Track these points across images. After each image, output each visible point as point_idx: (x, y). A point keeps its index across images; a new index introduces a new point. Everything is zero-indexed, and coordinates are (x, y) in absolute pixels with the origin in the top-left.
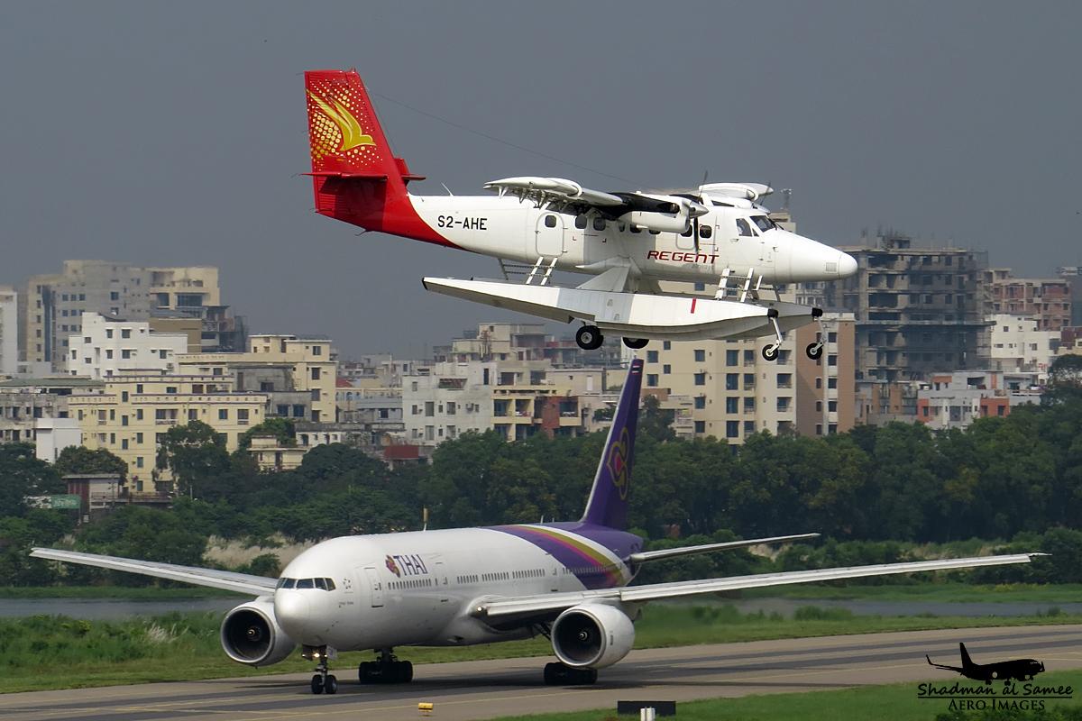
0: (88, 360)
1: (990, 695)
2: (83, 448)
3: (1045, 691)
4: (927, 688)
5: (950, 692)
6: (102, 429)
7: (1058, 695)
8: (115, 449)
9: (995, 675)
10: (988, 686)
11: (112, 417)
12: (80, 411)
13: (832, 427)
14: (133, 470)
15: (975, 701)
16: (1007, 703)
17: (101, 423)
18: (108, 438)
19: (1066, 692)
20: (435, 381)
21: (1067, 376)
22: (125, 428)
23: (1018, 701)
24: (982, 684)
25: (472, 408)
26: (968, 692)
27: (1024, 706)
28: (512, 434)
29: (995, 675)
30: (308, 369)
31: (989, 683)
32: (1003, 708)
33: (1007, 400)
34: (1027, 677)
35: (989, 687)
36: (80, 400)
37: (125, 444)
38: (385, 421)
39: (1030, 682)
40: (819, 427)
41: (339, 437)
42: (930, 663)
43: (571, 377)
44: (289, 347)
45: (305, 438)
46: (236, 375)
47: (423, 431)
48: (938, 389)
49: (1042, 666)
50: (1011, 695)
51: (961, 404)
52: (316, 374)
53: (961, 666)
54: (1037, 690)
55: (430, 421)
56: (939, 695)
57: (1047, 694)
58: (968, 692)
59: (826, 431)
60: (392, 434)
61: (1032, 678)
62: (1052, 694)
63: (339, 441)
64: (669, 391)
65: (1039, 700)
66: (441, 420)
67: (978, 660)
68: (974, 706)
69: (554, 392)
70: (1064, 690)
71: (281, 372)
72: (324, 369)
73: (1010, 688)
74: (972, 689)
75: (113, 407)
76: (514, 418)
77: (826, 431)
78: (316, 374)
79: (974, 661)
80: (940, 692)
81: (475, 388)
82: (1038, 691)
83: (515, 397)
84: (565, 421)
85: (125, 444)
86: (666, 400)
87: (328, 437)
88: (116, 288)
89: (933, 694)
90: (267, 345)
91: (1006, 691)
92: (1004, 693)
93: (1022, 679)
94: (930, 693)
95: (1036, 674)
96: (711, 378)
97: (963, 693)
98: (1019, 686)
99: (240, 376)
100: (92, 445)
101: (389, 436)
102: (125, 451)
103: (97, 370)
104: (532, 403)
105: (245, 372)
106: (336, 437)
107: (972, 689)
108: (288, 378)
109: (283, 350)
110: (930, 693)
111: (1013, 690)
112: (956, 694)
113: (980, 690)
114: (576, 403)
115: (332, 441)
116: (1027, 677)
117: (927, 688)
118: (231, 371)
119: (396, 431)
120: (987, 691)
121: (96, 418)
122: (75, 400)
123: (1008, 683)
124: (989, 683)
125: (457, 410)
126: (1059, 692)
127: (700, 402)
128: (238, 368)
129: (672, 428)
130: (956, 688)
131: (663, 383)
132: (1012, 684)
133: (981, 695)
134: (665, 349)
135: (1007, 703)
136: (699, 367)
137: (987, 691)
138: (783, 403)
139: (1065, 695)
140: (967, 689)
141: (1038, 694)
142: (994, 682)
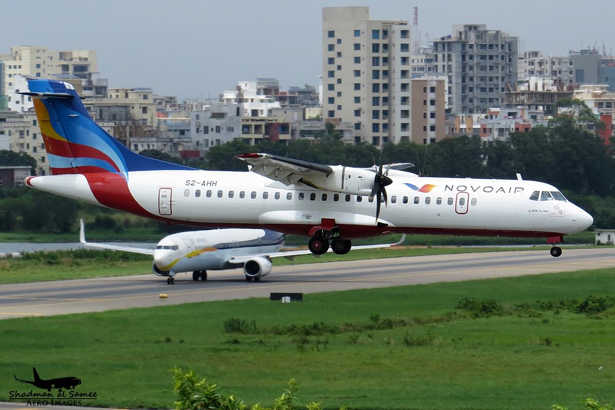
0: (18, 102)
1: (50, 397)
2: (11, 151)
3: (81, 395)
4: (14, 394)
5: (28, 395)
6: (22, 141)
7: (89, 397)
8: (30, 152)
9: (53, 386)
10: (49, 392)
11: (28, 134)
12: (10, 131)
13: (433, 140)
14: (39, 164)
16: (60, 402)
17: (21, 138)
18: (25, 146)
20: (209, 114)
21: (562, 111)
22: (35, 140)
24: (46, 391)
25: (231, 129)
26: (38, 396)
28: (253, 143)
29: (53, 386)
30: (140, 107)
31: (49, 390)
33: (530, 125)
34: (71, 387)
35: (50, 393)
36: (10, 125)
37: (35, 149)
38: (182, 136)
39: (73, 390)
40: (425, 141)
41: (155, 146)
43: (285, 112)
44: (130, 96)
45: (136, 146)
46: (98, 111)
47: (203, 143)
48: (491, 118)
49: (80, 381)
50: (62, 397)
51: (504, 127)
52: (145, 110)
53: (34, 381)
54: (77, 394)
55: (206, 136)
56: (21, 397)
57: (83, 397)
59: (429, 142)
60: (185, 144)
61: (74, 388)
62: (86, 397)
63: (155, 148)
64: (340, 120)
65: (79, 400)
66: (212, 136)
67: (43, 377)
69: (276, 120)
71: (124, 109)
72: (149, 107)
73: (62, 393)
74: (40, 394)
75: (28, 129)
76: (253, 136)
77: (429, 142)
78: (145, 110)
80: (22, 395)
81: (232, 118)
83: (254, 123)
84: (282, 137)
85: (35, 149)
86: (338, 124)
87: (149, 146)
88: (40, 61)
89: (18, 397)
90: (117, 94)
92: (58, 396)
93: (68, 388)
95: (76, 385)
96: (364, 112)
98: (66, 392)
99: (101, 111)
100: (16, 150)
101: (182, 145)
102: (35, 154)
103: (23, 108)
104: (264, 127)
105: (104, 109)
106: (153, 146)
107: (40, 394)
108: (127, 113)
109: (127, 96)
111: (63, 395)
112: (31, 397)
113: (45, 394)
114: (288, 127)
115: (151, 148)
117: (14, 394)
118: (95, 108)
119: (187, 142)
120: (49, 395)
121: (18, 135)
122: (6, 125)
124: (49, 390)
125: (221, 131)
126: (90, 395)
127: (358, 126)
128: (99, 107)
129: (342, 141)
130: (31, 393)
131: (338, 114)
132: (63, 391)
133: (45, 397)
134: (338, 96)
136: (357, 106)
137: (49, 395)
138: (404, 126)
139: (93, 397)
140: (37, 394)
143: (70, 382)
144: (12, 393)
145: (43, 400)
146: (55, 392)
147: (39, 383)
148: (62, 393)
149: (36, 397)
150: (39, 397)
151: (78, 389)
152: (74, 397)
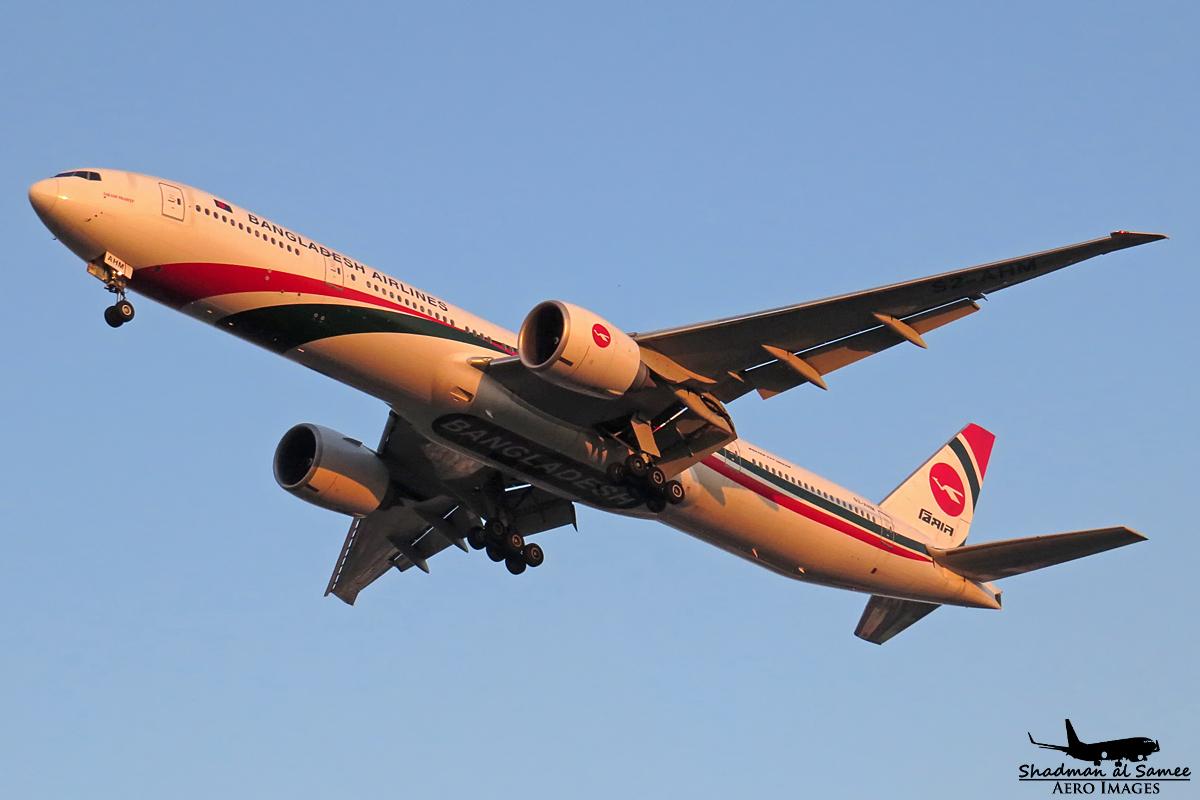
1: (1099, 777)
3: (1159, 773)
4: (1029, 770)
5: (1055, 774)
7: (1174, 777)
9: (1104, 755)
10: (1097, 767)
15: (1082, 783)
16: (1117, 787)
19: (1184, 774)
23: (1130, 784)
24: (1090, 764)
26: (1075, 774)
27: (1137, 788)
29: (1104, 755)
31: (1097, 763)
32: (1113, 791)
34: (1140, 757)
35: (1098, 768)
39: (1143, 763)
42: (1032, 741)
49: (1157, 745)
50: (1123, 777)
53: (1067, 745)
54: (1151, 771)
56: (1042, 777)
57: (1162, 776)
58: (1075, 774)
61: (1145, 759)
62: (1168, 776)
65: (1153, 783)
67: (1086, 738)
68: (1081, 789)
70: (1181, 772)
73: (1122, 769)
74: (1079, 771)
79: (1081, 740)
80: (1043, 774)
82: (1152, 773)
89: (1036, 776)
91: (1116, 773)
92: (1114, 775)
93: (1135, 759)
94: (1032, 775)
97: (1069, 775)
98: (1131, 767)
107: (1079, 771)
110: (1032, 775)
111: (1124, 772)
112: (1061, 777)
113: (1088, 771)
116: (1140, 757)
117: (1029, 770)
120: (1096, 773)
123: (1119, 764)
124: (1097, 763)
126: (1176, 774)
130: (1062, 769)
132: (1123, 765)
133: (1089, 777)
135: (1117, 787)
137: (1096, 773)
139: (1182, 777)
141: (1152, 777)
142: (1103, 762)
143: (1138, 748)
144: (1024, 769)
145: (1086, 782)
146: (1108, 766)
147: (1076, 748)
148: (1122, 769)
149: (1072, 777)
150: (1078, 776)
151: (1153, 761)
152: (1145, 777)
